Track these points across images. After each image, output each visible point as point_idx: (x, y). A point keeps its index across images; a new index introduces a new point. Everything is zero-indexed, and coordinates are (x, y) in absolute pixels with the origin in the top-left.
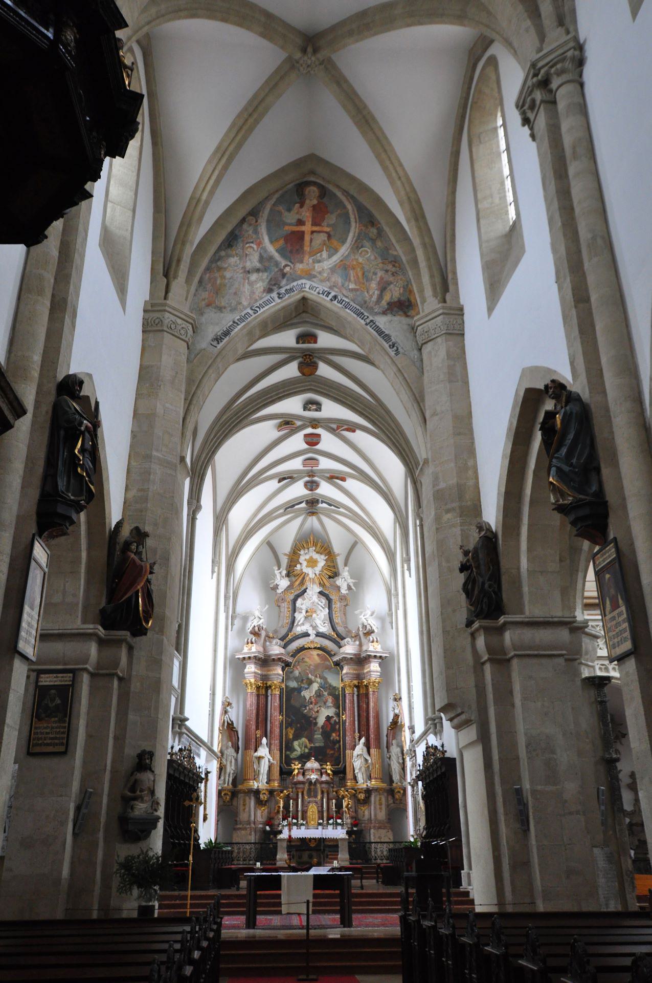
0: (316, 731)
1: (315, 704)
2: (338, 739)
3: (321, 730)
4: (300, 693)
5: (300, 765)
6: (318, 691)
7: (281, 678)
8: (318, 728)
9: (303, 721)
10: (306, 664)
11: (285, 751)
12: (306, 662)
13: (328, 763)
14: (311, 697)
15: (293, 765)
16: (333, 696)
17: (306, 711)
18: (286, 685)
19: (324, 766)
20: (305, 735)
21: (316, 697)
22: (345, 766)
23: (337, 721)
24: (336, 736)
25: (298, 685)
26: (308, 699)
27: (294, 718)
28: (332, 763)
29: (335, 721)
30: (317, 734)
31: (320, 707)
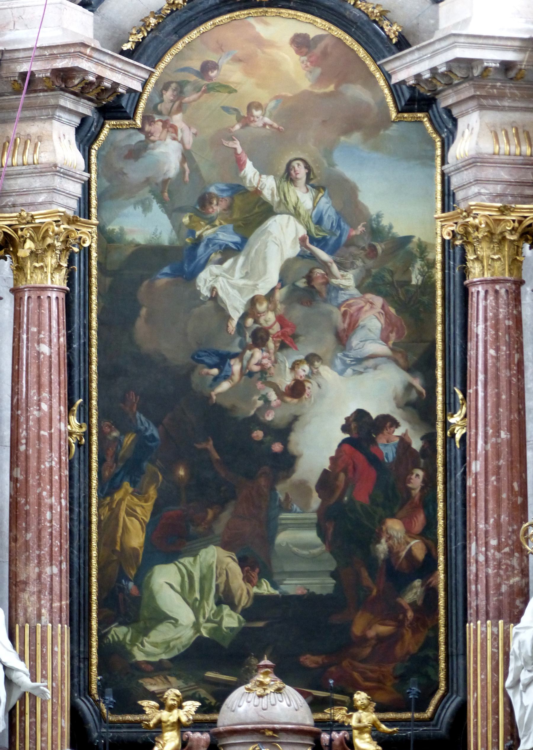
0: (286, 507)
1: (283, 346)
2: (420, 553)
3: (316, 501)
4: (193, 276)
5: (191, 706)
6: (304, 267)
7: (77, 189)
8: (302, 485)
9: (210, 445)
10: (224, 99)
11: (103, 623)
12: (229, 89)
13: (361, 697)
14: (254, 301)
15: (147, 704)
16: (384, 295)
17: (225, 386)
18: (101, 229)
19: (340, 714)
20: (219, 528)
21: (289, 300)
22: (462, 709)
23: (417, 444)
24: (409, 532)
25: (177, 227)
26: (236, 316)
27: (153, 431)
28: (384, 697)
29: (404, 443)
30: (300, 525)
31: (310, 359)
